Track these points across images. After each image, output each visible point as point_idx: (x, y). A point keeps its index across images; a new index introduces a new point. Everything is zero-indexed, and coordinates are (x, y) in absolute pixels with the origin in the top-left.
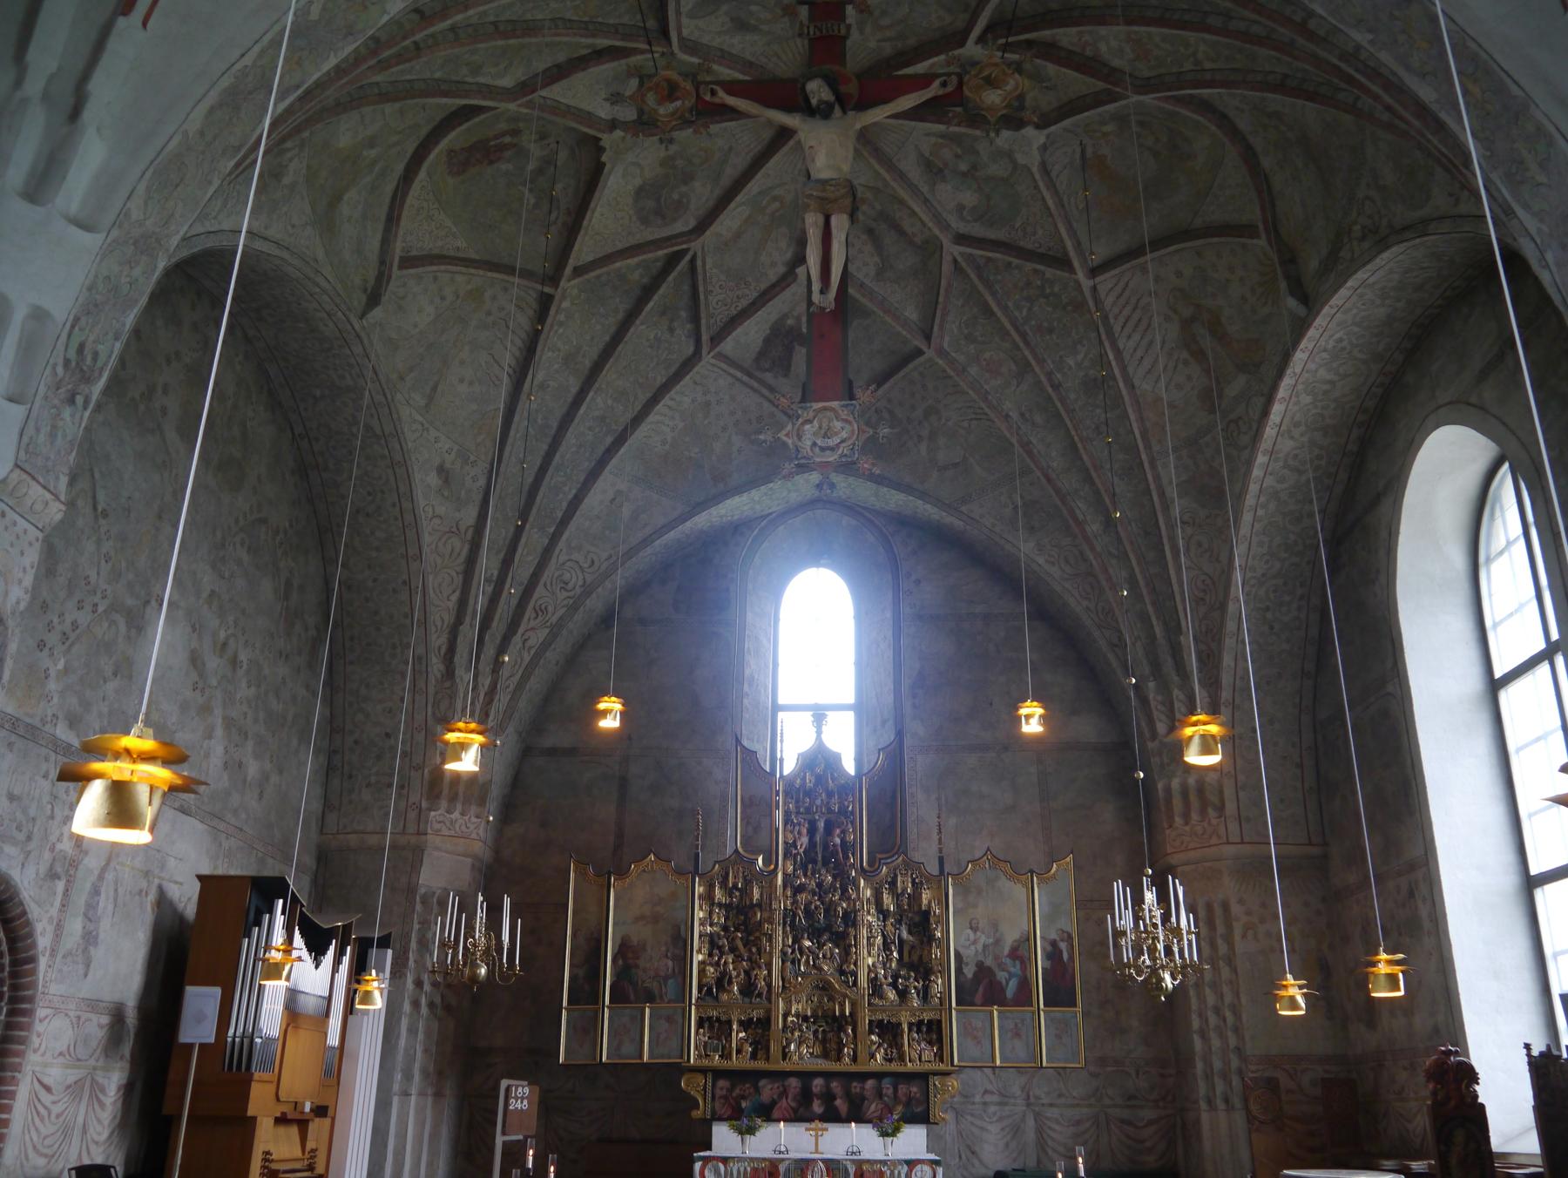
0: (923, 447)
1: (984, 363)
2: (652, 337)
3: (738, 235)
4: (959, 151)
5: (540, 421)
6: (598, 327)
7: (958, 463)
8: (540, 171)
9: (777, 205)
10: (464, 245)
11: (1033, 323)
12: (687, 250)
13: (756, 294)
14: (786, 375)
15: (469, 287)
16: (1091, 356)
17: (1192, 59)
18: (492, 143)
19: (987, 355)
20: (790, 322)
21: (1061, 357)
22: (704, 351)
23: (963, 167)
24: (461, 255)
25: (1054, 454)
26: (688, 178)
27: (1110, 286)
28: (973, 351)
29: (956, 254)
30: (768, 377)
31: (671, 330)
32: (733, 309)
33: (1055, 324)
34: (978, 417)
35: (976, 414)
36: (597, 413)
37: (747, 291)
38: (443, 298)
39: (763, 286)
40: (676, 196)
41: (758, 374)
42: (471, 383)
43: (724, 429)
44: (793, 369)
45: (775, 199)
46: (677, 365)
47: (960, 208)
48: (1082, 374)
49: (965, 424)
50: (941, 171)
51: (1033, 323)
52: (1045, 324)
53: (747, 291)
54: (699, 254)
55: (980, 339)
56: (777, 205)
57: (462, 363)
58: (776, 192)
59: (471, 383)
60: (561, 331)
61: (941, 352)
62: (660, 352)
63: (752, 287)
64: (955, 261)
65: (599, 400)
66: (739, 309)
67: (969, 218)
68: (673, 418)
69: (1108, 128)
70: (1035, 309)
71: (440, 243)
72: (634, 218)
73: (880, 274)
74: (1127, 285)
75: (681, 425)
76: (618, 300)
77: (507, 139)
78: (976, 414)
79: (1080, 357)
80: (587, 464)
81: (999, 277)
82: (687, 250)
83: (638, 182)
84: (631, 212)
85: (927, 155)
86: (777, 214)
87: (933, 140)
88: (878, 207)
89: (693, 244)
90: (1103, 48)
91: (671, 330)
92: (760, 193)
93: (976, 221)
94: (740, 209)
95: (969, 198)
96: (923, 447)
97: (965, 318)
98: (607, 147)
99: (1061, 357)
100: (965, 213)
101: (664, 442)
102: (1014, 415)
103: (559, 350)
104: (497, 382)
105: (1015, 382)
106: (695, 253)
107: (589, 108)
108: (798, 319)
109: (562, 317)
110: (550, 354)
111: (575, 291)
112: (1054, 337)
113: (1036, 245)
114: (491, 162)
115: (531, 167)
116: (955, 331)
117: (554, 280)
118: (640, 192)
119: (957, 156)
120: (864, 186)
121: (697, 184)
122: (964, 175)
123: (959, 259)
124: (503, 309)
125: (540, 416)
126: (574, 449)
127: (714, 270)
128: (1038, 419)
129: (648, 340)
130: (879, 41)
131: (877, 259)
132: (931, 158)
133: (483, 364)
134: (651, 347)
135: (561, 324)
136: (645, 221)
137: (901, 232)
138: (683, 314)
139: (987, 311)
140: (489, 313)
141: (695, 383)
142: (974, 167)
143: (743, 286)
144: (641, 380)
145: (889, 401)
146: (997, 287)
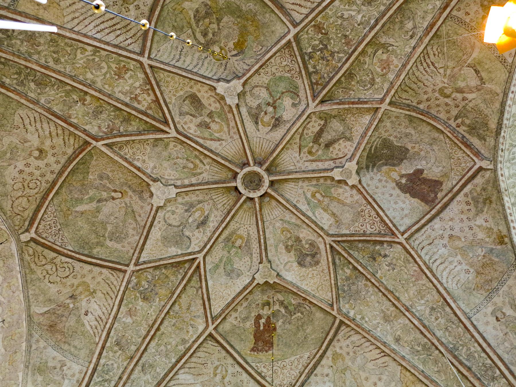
0: (470, 96)
1: (384, 70)
2: (388, 268)
3: (334, 214)
4: (263, 113)
5: (419, 349)
6: (373, 297)
7: (475, 70)
8: (286, 308)
9: (318, 195)
10: (308, 354)
11: (346, 48)
12: (330, 244)
13: (369, 207)
14: (441, 183)
15: (330, 359)
16: (347, 7)
17: (97, 54)
18: (262, 328)
19: (379, 70)
20: (404, 181)
21: (359, 25)
22: (397, 240)
23: (270, 109)
24: (311, 357)
25: (430, 7)
26: (298, 240)
27: (297, 14)
28: (379, 79)
29: (315, 104)
30: (440, 195)
31: (385, 256)
32: (377, 220)
33: (340, 35)
34: (430, 64)
35: (428, 66)
36: (428, 311)
37: (367, 211)
38: (327, 375)
39: (364, 202)
40: (307, 246)
41: (437, 201)
42: (380, 379)
43: (471, 228)
44: (437, 179)
45: (313, 196)
46: (408, 256)
47: (294, 105)
48: (364, 8)
49: (442, 71)
50: (277, 119)
51: (346, 48)
52: (343, 41)
53: (367, 211)
54: (333, 239)
55: (370, 77)
56: (318, 195)
57: (367, 379)
58: (309, 195)
59: (380, 379)
60: (367, 319)
61: (382, 100)
62: (398, 264)
63: (364, 208)
64: (322, 102)
65: (419, 308)
66: (377, 217)
67: (298, 99)
68: (451, 263)
69: (217, 49)
70: (337, 50)
71: (300, 366)
72: (314, 268)
73: (349, 139)
74: (293, 4)
75: (459, 257)
76: (360, 283)
77: (263, 321)
78: (428, 66)
79: (353, 13)
80: (460, 329)
81: (326, 75)
82: (330, 244)
83: (295, 264)
84: (310, 269)
85: (270, 128)
86: (323, 194)
87: (260, 126)
88: (311, 144)
89: (327, 242)
90: (137, 84)
91: (385, 256)
92: (309, 204)
93: (298, 96)
94: (317, 214)
95: (287, 102)
96: (470, 96)
97: (361, 88)
98: (265, 280)
99: (359, 25)
100: (296, 102)
101: (467, 272)
102: (413, 42)
103: (379, 323)
104: (386, 364)
105: (390, 48)
106: (333, 241)
107: (243, 286)
108: (402, 176)
109: (358, 317)
110: (379, 329)
111: (347, 306)
112: (348, 33)
113: (293, 62)
114: (275, 329)
115: (283, 310)
116: (371, 92)
117: (335, 318)
118: (301, 264)
119: (266, 113)
120: (300, 152)
121: (301, 236)
122: (275, 108)
123: (317, 102)
124: (348, 345)
125: (416, 347)
126: (447, 334)
127: (351, 229)
128: (409, 25)
129: (389, 270)
130: (205, 165)
131: (341, 141)
132: (271, 125)
133: (374, 367)
134: (394, 269)
135: (363, 318)
136: (317, 263)
137: (321, 131)
138: (378, 247)
139: (350, 75)
140: (348, 354)
141: (429, 244)
142: (268, 104)
143: (363, 213)
144: (413, 279)
145: (449, 119)
146: (331, 75)
